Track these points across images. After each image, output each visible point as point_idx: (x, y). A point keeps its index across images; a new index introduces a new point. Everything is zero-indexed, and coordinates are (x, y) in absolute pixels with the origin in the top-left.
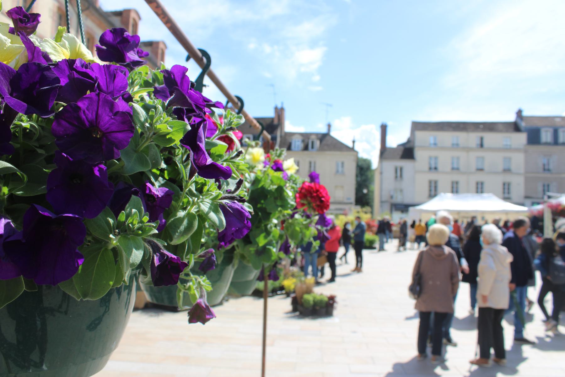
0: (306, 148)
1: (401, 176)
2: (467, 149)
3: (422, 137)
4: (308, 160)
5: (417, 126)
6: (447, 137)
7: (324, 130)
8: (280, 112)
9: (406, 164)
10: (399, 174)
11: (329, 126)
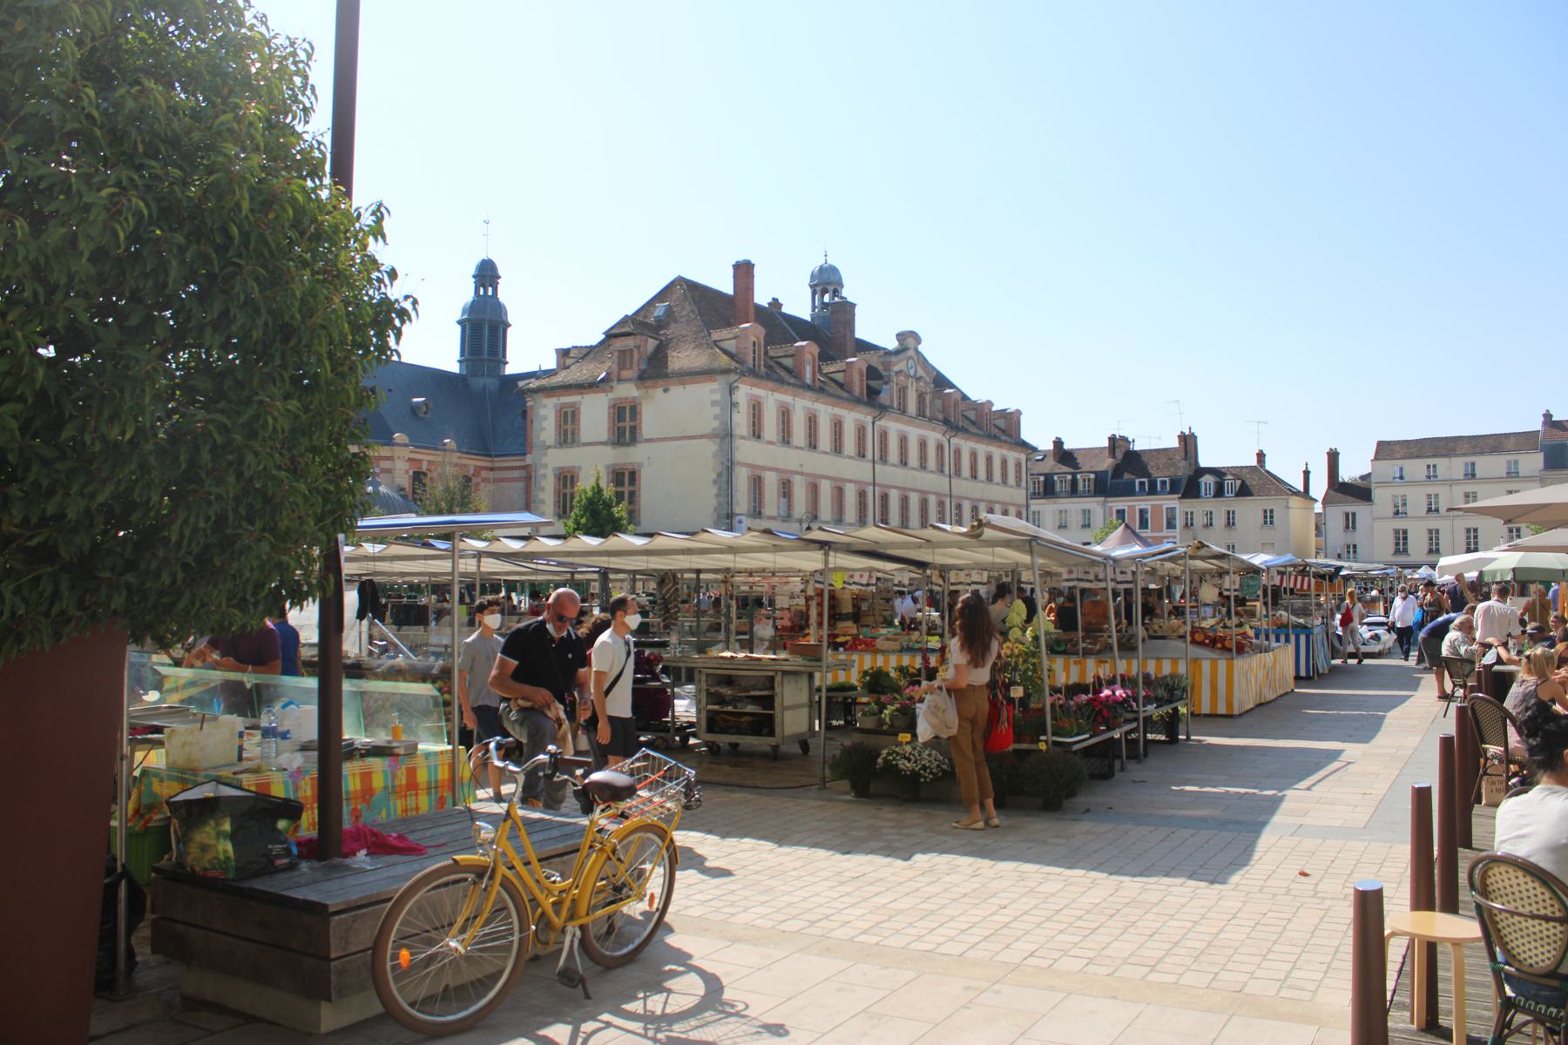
0: (1219, 492)
1: (1354, 527)
2: (1451, 482)
3: (1391, 468)
4: (1224, 509)
5: (1385, 450)
6: (1416, 468)
7: (1254, 462)
8: (1188, 442)
9: (1361, 510)
10: (1350, 522)
11: (1261, 456)
